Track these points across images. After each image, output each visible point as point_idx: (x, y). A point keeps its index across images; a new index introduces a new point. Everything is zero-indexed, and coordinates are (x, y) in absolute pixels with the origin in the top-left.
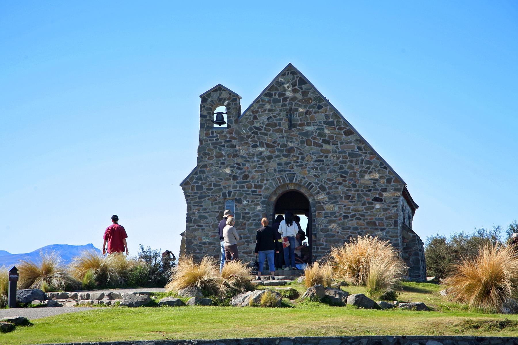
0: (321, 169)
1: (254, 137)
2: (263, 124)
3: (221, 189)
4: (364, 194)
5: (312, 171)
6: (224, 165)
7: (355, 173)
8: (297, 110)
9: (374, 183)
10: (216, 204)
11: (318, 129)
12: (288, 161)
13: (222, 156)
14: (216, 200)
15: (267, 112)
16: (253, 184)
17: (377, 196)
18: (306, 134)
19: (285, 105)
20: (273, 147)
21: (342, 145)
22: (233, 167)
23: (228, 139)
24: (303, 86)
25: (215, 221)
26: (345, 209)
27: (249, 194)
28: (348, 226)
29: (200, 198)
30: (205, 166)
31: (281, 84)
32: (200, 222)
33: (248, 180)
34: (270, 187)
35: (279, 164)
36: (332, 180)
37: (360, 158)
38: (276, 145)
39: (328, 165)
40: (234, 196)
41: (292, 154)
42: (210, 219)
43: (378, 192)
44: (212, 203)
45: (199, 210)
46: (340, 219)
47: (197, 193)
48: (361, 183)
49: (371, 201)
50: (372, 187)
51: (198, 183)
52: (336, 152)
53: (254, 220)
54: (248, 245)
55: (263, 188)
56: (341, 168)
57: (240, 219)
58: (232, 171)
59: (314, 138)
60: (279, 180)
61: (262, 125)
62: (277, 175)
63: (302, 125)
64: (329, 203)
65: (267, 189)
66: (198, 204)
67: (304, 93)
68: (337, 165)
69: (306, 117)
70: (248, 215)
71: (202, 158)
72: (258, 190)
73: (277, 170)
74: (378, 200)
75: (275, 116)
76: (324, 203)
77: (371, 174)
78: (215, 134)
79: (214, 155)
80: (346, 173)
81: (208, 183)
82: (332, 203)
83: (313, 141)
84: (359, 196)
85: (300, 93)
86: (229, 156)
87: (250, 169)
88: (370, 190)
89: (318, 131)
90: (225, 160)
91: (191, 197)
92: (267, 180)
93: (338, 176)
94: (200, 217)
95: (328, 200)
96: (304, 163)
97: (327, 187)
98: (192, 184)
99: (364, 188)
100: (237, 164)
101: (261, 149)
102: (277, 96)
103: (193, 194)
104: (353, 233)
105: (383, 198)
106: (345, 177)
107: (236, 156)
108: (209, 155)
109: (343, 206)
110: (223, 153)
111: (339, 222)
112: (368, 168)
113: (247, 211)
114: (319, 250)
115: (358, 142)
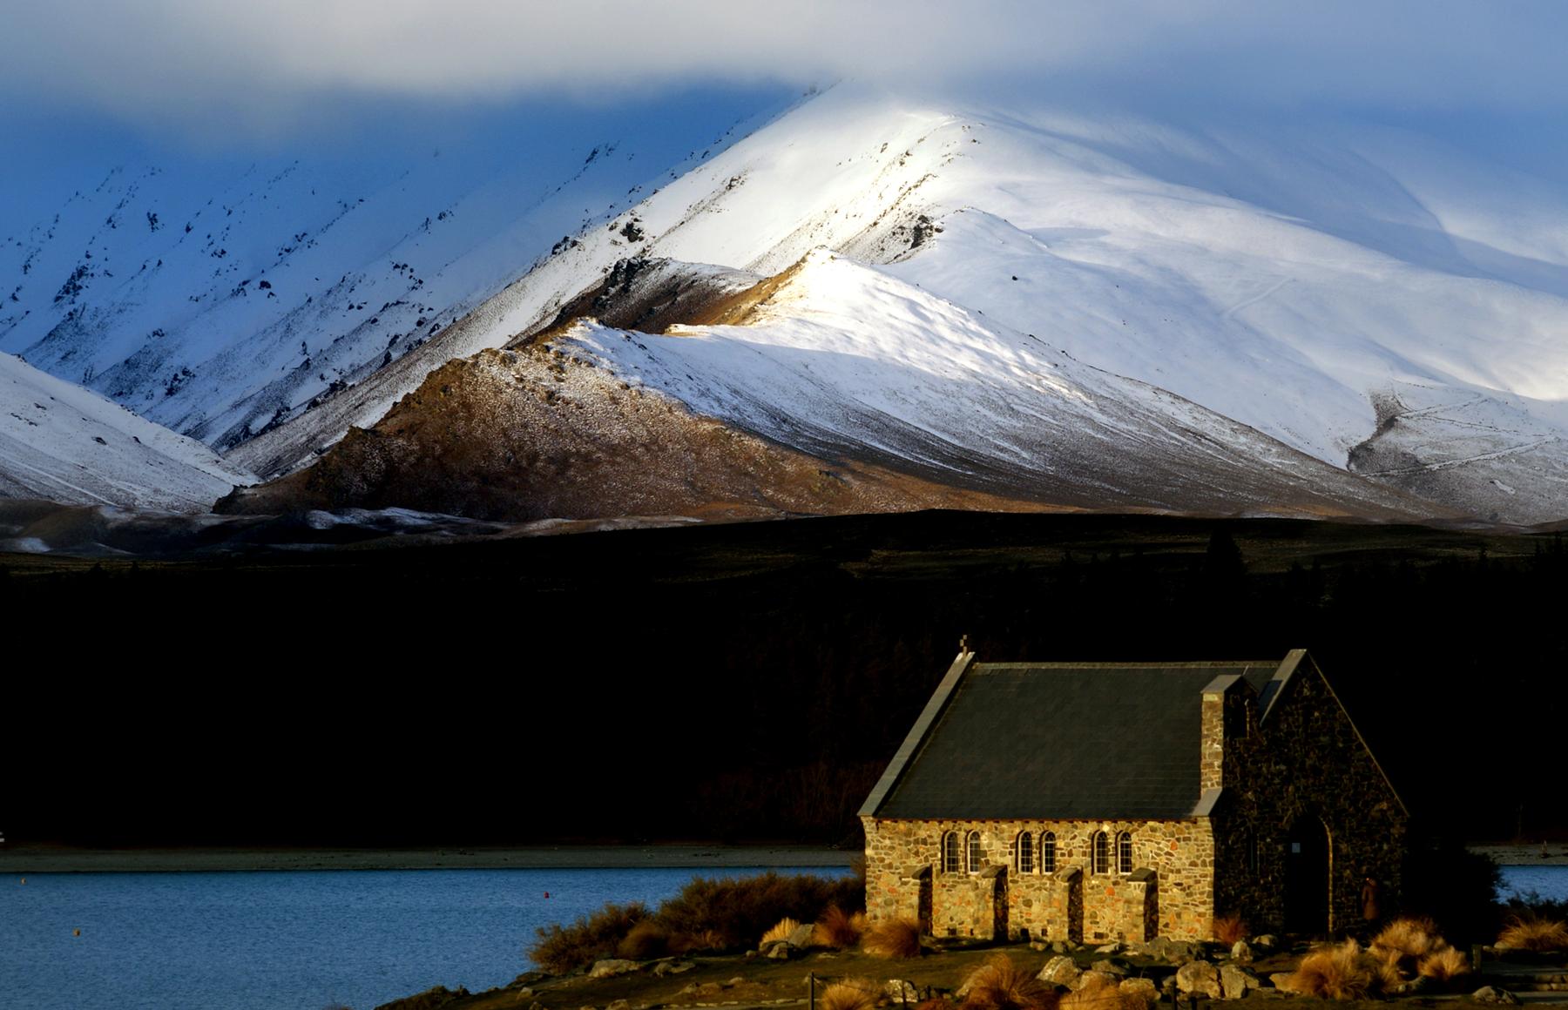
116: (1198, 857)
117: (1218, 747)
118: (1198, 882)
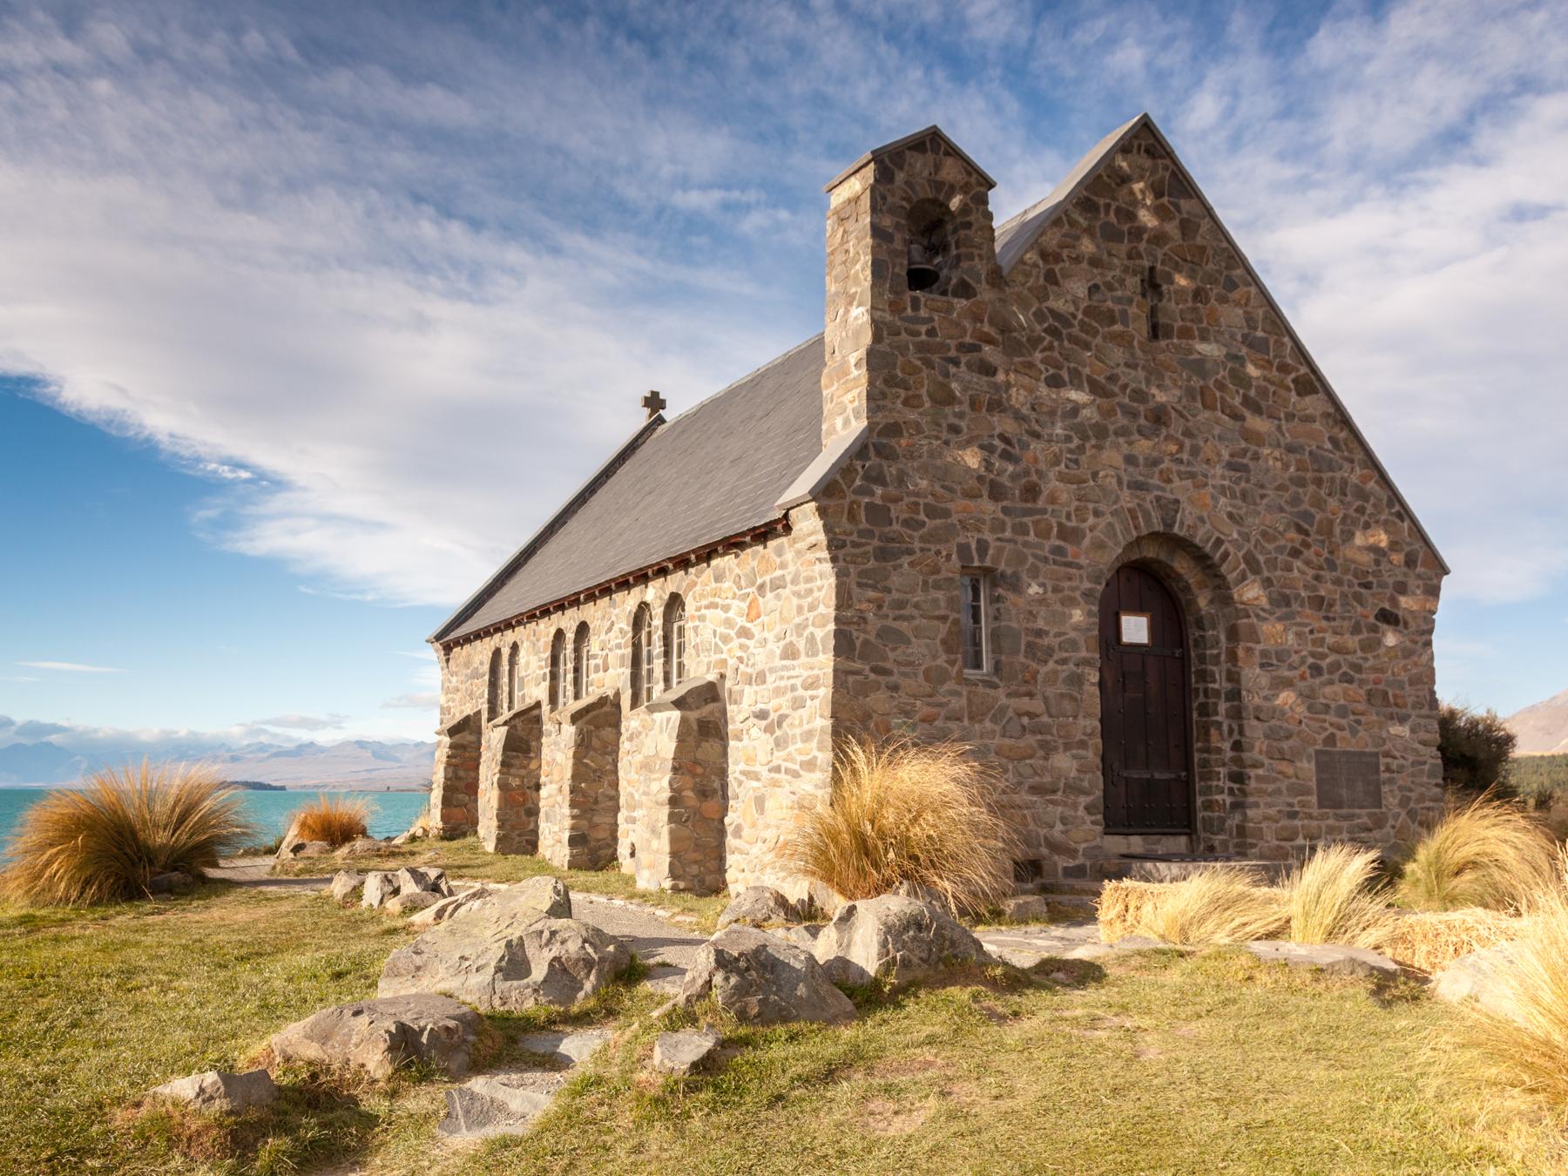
0: (1244, 495)
1: (1050, 348)
2: (1075, 302)
3: (950, 531)
4: (1358, 598)
5: (1223, 500)
6: (963, 437)
7: (1331, 522)
8: (1171, 282)
9: (1377, 563)
10: (937, 587)
11: (1227, 355)
12: (1155, 454)
13: (950, 399)
14: (936, 570)
15: (1085, 265)
16: (1054, 522)
17: (1387, 606)
18: (1199, 366)
19: (1140, 256)
20: (1113, 395)
21: (1291, 425)
22: (988, 449)
23: (968, 339)
24: (1185, 204)
25: (935, 657)
26: (1314, 642)
27: (1046, 560)
28: (1322, 700)
29: (882, 555)
30: (894, 430)
31: (1124, 180)
32: (885, 659)
33: (1040, 504)
34: (1103, 544)
35: (1130, 460)
36: (1275, 539)
37: (1338, 475)
38: (1116, 389)
39: (1262, 486)
40: (996, 559)
41: (1164, 431)
42: (918, 648)
43: (1389, 591)
44: (925, 583)
45: (880, 607)
46: (1303, 677)
47: (866, 534)
48: (1346, 560)
49: (1372, 620)
50: (1374, 574)
51: (872, 494)
52: (1279, 446)
53: (1064, 661)
54: (1046, 759)
55: (1086, 542)
56: (1295, 500)
57: (1017, 652)
58: (988, 465)
59: (1221, 386)
60: (1134, 518)
61: (1072, 309)
62: (1127, 499)
63: (1186, 333)
64: (1272, 618)
65: (1099, 546)
66: (869, 580)
67: (1187, 227)
68: (1281, 487)
69: (1195, 310)
70: (1046, 641)
71: (884, 395)
72: (1070, 548)
73: (1125, 479)
74: (1389, 618)
75: (1110, 287)
76: (1258, 616)
77: (1369, 532)
78: (923, 313)
79: (924, 392)
80: (1308, 517)
81: (907, 500)
82: (1279, 619)
83: (1218, 394)
84: (1345, 604)
85: (1176, 222)
86: (974, 404)
87: (1042, 466)
88: (1367, 586)
89: (1229, 365)
90: (961, 415)
91: (849, 549)
92: (1097, 514)
93: (1288, 525)
94: (884, 633)
95: (1267, 607)
96: (1198, 468)
97: (1261, 559)
98: (850, 497)
99: (1355, 576)
100: (1003, 438)
101: (1076, 395)
102: (1112, 218)
103: (855, 537)
104: (1341, 729)
105: (1400, 614)
106: (1307, 533)
107: (996, 406)
108: (907, 389)
109: (1307, 630)
110: (954, 385)
111: (1301, 685)
112: (1361, 510)
113: (1040, 624)
114: (1253, 784)
115: (1331, 422)
116: (800, 628)
117: (860, 315)
118: (798, 704)
